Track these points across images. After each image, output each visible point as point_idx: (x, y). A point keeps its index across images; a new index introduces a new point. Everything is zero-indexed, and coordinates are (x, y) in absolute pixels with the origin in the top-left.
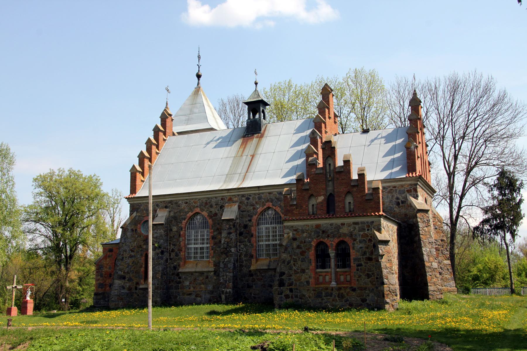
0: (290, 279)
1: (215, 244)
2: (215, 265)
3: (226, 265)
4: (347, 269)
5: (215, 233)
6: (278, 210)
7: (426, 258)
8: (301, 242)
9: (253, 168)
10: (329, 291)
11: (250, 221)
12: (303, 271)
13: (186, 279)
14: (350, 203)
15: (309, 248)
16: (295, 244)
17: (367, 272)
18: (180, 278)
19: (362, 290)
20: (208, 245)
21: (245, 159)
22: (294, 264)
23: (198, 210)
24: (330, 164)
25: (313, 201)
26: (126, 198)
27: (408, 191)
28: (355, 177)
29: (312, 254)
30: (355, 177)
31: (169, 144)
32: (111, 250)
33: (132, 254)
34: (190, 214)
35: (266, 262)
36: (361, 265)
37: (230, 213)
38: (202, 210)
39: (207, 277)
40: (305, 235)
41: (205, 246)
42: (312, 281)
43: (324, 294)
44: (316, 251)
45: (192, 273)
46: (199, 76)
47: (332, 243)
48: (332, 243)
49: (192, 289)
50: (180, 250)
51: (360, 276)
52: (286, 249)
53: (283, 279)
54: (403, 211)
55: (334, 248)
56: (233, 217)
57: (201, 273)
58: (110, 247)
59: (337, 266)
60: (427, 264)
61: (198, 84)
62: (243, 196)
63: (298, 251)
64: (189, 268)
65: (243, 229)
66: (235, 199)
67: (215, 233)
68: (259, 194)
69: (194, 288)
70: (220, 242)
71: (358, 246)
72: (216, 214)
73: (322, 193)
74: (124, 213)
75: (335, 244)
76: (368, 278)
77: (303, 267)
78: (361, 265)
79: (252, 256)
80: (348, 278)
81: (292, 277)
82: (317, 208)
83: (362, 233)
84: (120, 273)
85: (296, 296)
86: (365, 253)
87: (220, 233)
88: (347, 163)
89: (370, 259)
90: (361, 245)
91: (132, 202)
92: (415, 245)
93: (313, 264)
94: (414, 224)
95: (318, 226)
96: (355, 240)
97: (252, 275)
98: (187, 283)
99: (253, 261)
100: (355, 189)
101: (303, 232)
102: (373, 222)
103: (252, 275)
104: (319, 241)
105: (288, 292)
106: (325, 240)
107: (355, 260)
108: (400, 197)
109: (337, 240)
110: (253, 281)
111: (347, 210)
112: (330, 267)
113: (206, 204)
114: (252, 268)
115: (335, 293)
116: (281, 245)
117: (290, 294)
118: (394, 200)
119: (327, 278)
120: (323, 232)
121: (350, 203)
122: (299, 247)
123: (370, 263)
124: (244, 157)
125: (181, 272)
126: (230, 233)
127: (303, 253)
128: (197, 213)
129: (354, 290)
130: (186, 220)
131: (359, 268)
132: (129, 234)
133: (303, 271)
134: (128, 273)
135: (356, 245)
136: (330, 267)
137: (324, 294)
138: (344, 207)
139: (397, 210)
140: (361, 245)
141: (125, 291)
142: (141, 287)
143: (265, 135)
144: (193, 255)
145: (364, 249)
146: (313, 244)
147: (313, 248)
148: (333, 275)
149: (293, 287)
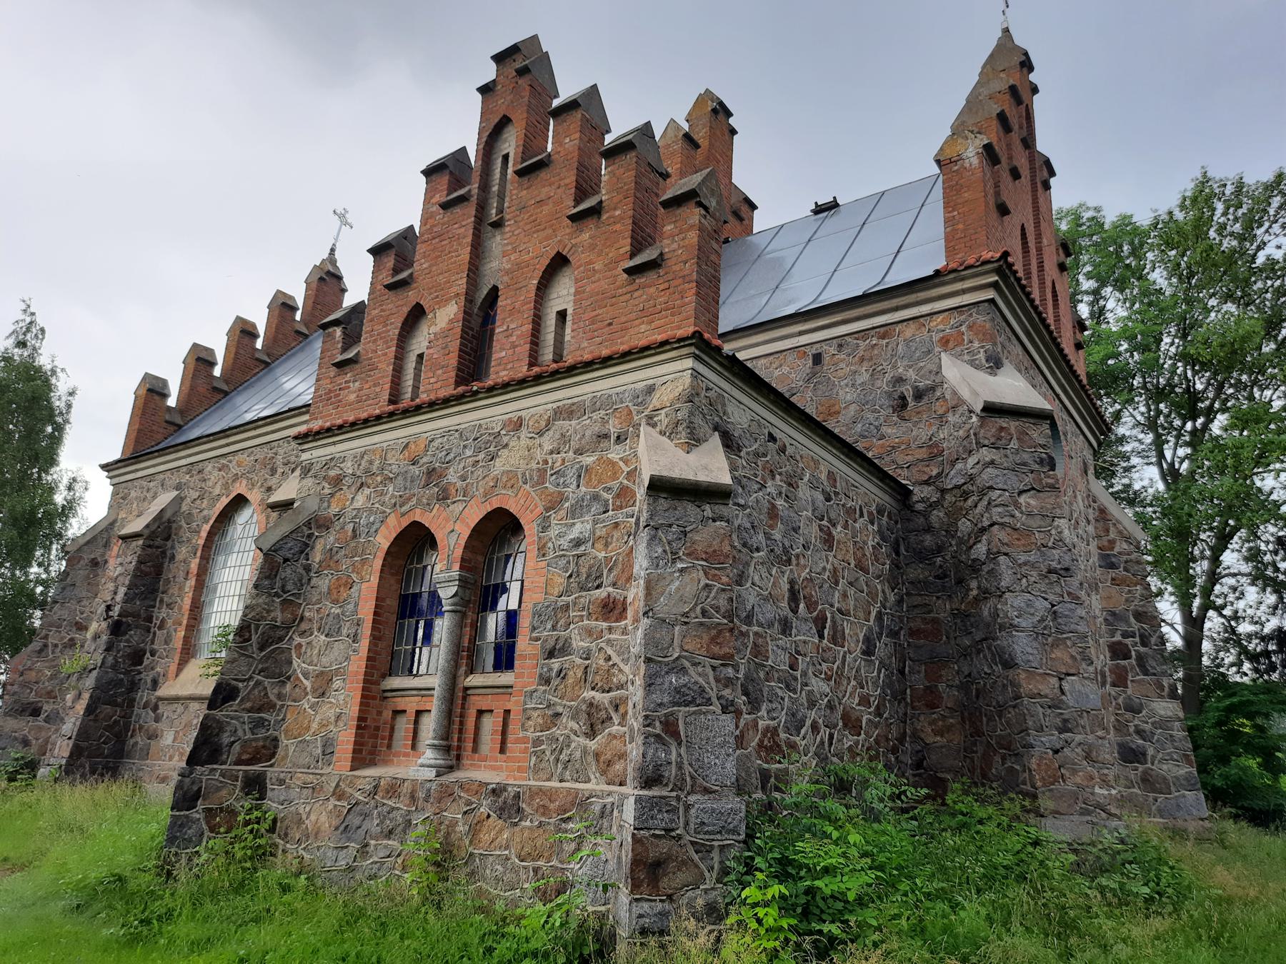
0: (260, 724)
7: (1022, 646)
14: (562, 315)
15: (364, 561)
17: (588, 694)
19: (544, 810)
22: (300, 645)
24: (506, 157)
34: (225, 501)
42: (346, 738)
48: (453, 529)
53: (221, 727)
54: (922, 433)
55: (459, 552)
73: (455, 289)
75: (464, 531)
76: (592, 733)
81: (270, 717)
83: (588, 460)
90: (580, 528)
91: (116, 480)
92: (974, 584)
94: (972, 478)
100: (586, 235)
102: (651, 390)
104: (405, 523)
108: (911, 374)
109: (475, 514)
111: (547, 354)
118: (883, 384)
121: (562, 315)
125: (160, 699)
130: (211, 522)
131: (555, 664)
135: (552, 533)
146: (383, 540)
147: (378, 563)
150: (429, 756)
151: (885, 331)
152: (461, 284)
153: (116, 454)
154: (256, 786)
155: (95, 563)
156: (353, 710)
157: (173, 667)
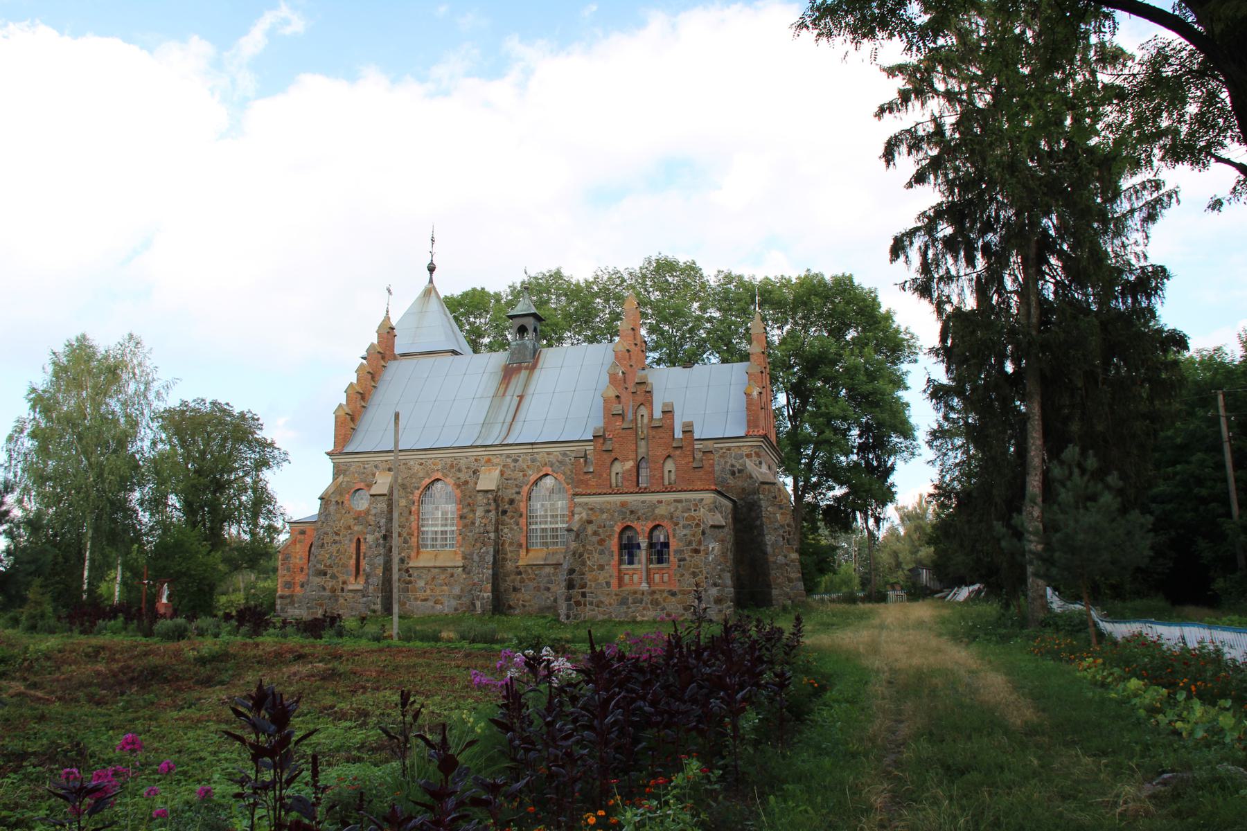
1: (465, 526)
2: (464, 558)
3: (482, 558)
4: (664, 565)
5: (465, 511)
6: (561, 477)
7: (769, 549)
8: (600, 527)
9: (521, 415)
10: (639, 596)
11: (518, 493)
12: (601, 568)
13: (420, 577)
16: (590, 529)
18: (410, 576)
20: (454, 528)
21: (510, 401)
23: (439, 475)
25: (617, 467)
26: (328, 454)
27: (747, 456)
28: (678, 434)
29: (614, 543)
30: (678, 434)
31: (397, 372)
32: (303, 532)
33: (337, 538)
34: (428, 481)
35: (542, 554)
36: (684, 560)
37: (489, 480)
38: (445, 476)
39: (452, 576)
40: (605, 516)
41: (449, 528)
42: (614, 581)
43: (630, 600)
44: (620, 538)
45: (429, 569)
46: (431, 269)
47: (643, 528)
48: (643, 528)
49: (429, 592)
50: (411, 534)
51: (683, 575)
52: (577, 536)
54: (740, 483)
56: (493, 487)
57: (444, 569)
58: (301, 527)
59: (650, 561)
60: (772, 559)
61: (431, 281)
62: (508, 456)
63: (595, 539)
64: (424, 560)
65: (504, 506)
66: (495, 461)
67: (465, 511)
68: (532, 454)
69: (432, 590)
70: (473, 523)
71: (681, 532)
72: (466, 483)
74: (322, 476)
77: (602, 562)
78: (684, 560)
79: (520, 546)
80: (666, 577)
82: (623, 477)
84: (318, 566)
85: (591, 604)
86: (690, 543)
87: (473, 511)
88: (668, 412)
89: (697, 551)
90: (685, 532)
93: (616, 558)
95: (623, 504)
96: (676, 524)
97: (520, 573)
98: (421, 583)
99: (523, 552)
100: (678, 452)
101: (602, 511)
103: (520, 573)
105: (580, 598)
106: (634, 524)
107: (676, 552)
109: (651, 525)
110: (522, 581)
111: (666, 483)
112: (640, 562)
113: (452, 466)
114: (520, 563)
115: (647, 599)
116: (569, 530)
117: (582, 600)
118: (728, 467)
119: (636, 577)
120: (632, 512)
122: (595, 533)
123: (697, 557)
124: (508, 398)
126: (488, 511)
127: (601, 542)
128: (438, 480)
129: (673, 594)
132: (332, 508)
133: (601, 568)
134: (330, 566)
136: (640, 562)
137: (630, 600)
138: (662, 478)
139: (731, 482)
140: (685, 532)
141: (327, 593)
142: (351, 587)
143: (540, 365)
144: (429, 542)
145: (689, 537)
146: (617, 529)
148: (644, 574)
149: (586, 590)
150: (644, 584)
151: (729, 449)
152: (632, 456)
153: (331, 448)
154: (584, 595)
155: (337, 502)
156: (615, 574)
157: (413, 554)
